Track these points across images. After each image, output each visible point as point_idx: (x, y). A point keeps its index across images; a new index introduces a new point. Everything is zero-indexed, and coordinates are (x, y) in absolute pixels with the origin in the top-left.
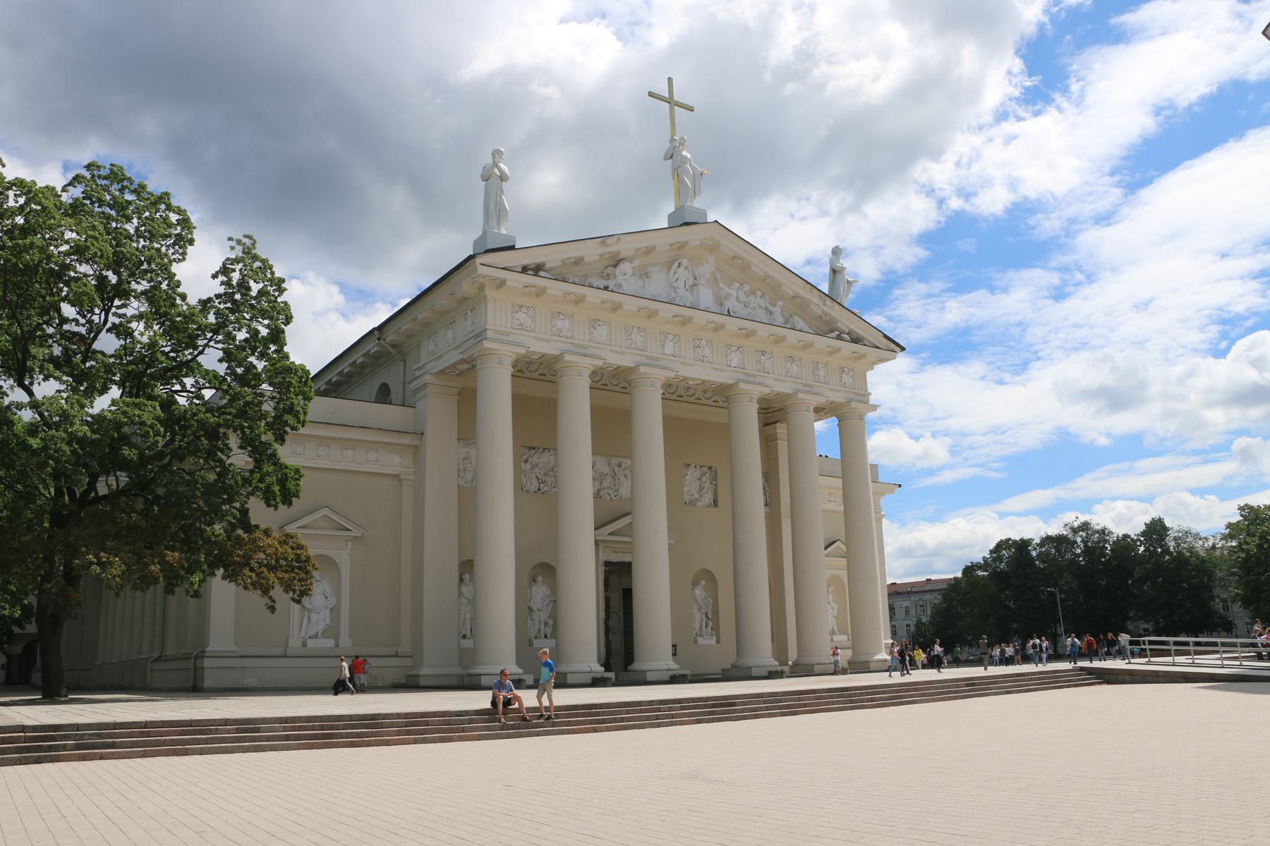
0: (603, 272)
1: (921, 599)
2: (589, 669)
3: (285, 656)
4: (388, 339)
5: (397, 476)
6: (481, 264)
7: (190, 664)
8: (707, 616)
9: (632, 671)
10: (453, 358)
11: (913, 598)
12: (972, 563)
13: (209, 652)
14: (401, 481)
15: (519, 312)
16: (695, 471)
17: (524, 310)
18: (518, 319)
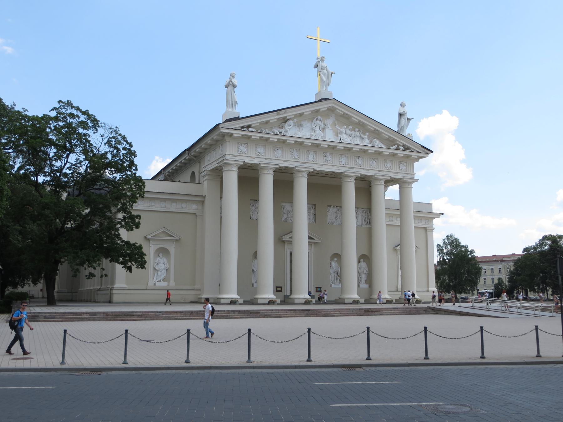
0: (280, 126)
1: (507, 264)
2: (268, 297)
3: (146, 289)
4: (192, 154)
5: (195, 214)
6: (222, 128)
7: (108, 292)
8: (337, 274)
9: (291, 298)
10: (215, 165)
11: (503, 264)
12: (529, 246)
13: (115, 287)
14: (197, 216)
15: (241, 146)
16: (334, 209)
17: (243, 145)
18: (240, 149)
